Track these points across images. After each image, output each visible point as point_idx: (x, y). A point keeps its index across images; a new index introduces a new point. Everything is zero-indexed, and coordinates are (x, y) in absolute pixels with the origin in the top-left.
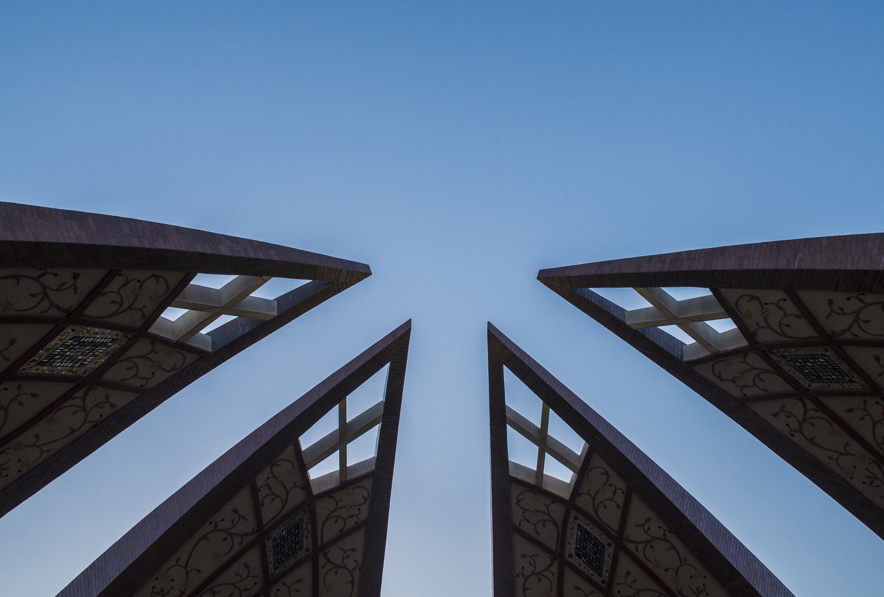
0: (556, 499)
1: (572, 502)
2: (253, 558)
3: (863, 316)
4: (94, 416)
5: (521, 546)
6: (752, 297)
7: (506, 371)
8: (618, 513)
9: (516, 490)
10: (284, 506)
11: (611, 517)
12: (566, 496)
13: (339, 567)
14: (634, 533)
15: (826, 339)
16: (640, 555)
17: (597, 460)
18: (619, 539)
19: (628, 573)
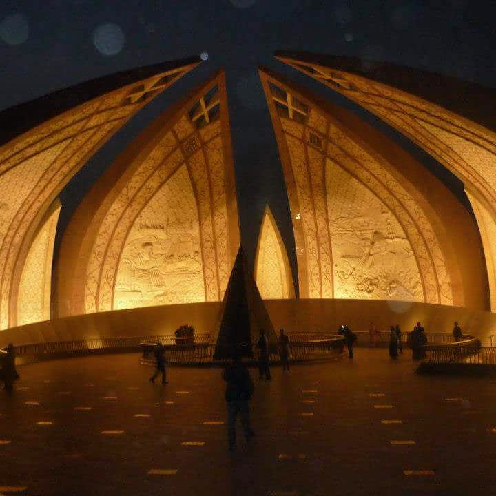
2: (178, 152)
4: (109, 129)
5: (288, 138)
11: (323, 130)
13: (212, 149)
18: (326, 136)
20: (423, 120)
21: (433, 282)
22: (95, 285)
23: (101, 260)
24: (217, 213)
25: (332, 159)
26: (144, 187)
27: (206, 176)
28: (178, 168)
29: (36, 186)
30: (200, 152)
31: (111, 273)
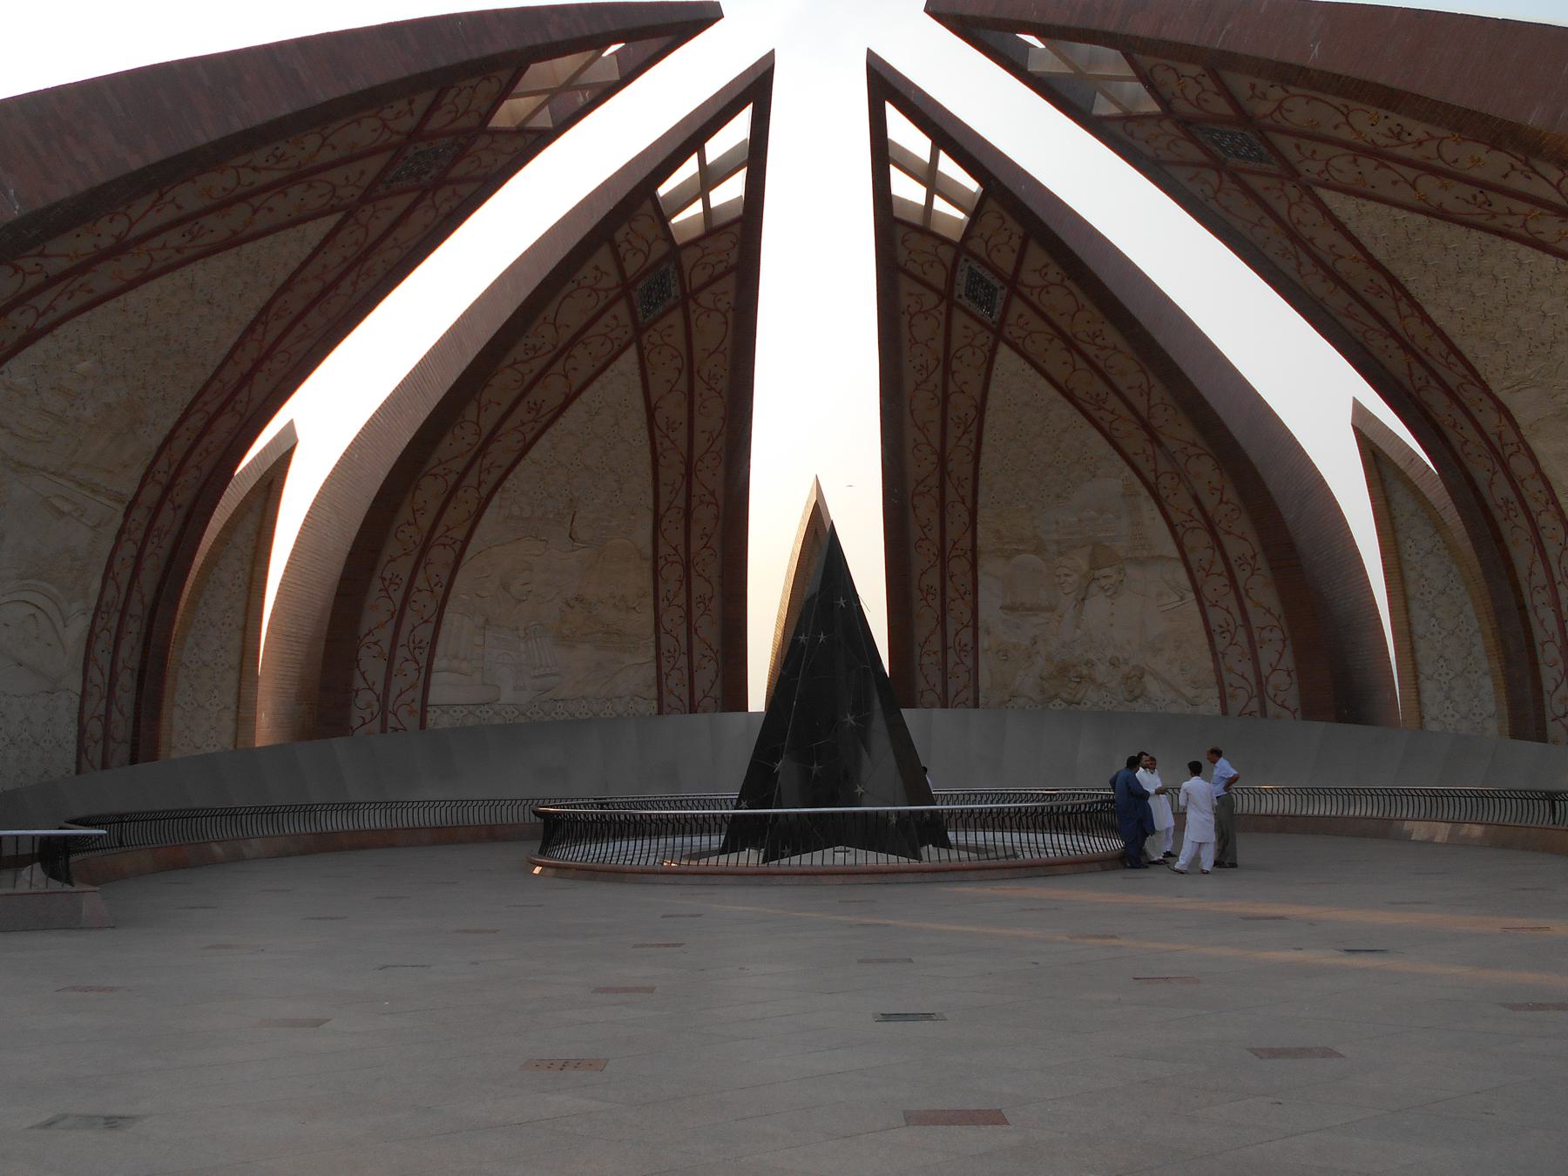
0: (945, 241)
1: (963, 246)
2: (621, 309)
3: (1287, 105)
4: (445, 208)
5: (906, 284)
6: (1169, 68)
7: (891, 111)
8: (1014, 257)
9: (900, 231)
10: (647, 258)
11: (1006, 261)
12: (957, 238)
14: (1029, 277)
15: (1244, 118)
16: (1034, 299)
17: (991, 204)
18: (1013, 283)
19: (1021, 316)
20: (1347, 191)
21: (1246, 668)
22: (383, 665)
23: (398, 597)
24: (697, 490)
25: (1014, 347)
26: (522, 408)
27: (683, 384)
28: (615, 358)
29: (229, 357)
30: (676, 318)
31: (425, 632)
